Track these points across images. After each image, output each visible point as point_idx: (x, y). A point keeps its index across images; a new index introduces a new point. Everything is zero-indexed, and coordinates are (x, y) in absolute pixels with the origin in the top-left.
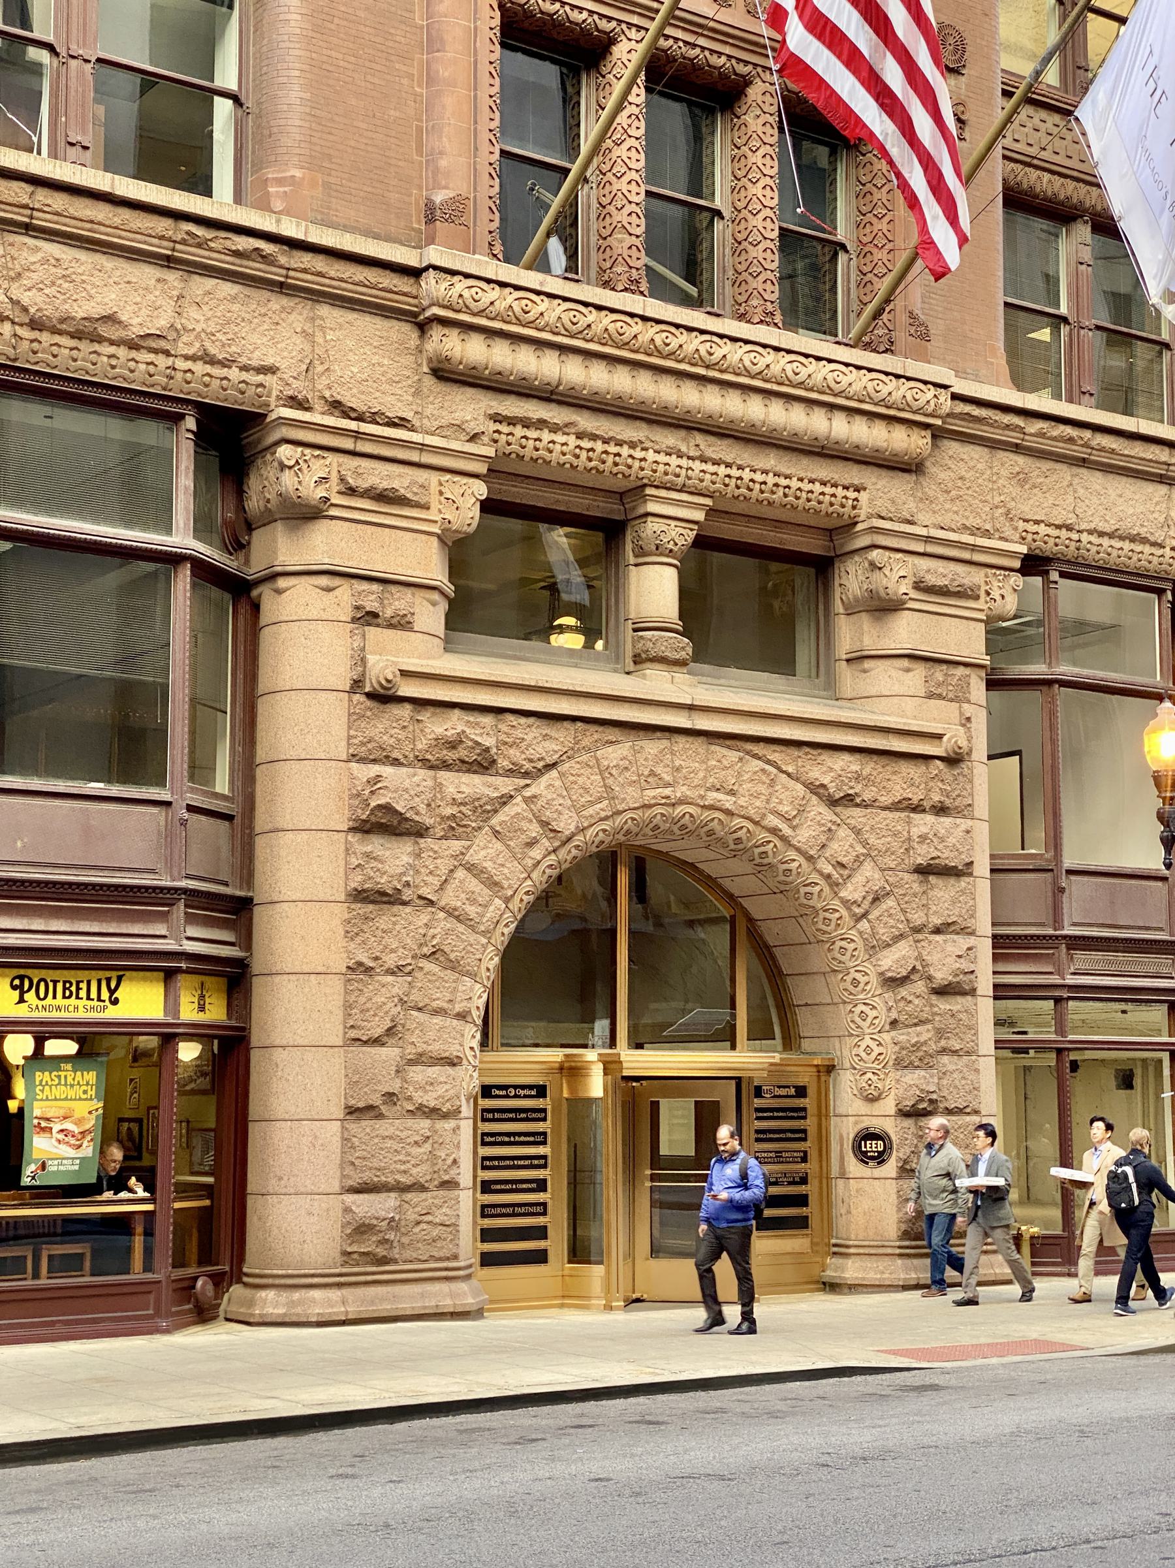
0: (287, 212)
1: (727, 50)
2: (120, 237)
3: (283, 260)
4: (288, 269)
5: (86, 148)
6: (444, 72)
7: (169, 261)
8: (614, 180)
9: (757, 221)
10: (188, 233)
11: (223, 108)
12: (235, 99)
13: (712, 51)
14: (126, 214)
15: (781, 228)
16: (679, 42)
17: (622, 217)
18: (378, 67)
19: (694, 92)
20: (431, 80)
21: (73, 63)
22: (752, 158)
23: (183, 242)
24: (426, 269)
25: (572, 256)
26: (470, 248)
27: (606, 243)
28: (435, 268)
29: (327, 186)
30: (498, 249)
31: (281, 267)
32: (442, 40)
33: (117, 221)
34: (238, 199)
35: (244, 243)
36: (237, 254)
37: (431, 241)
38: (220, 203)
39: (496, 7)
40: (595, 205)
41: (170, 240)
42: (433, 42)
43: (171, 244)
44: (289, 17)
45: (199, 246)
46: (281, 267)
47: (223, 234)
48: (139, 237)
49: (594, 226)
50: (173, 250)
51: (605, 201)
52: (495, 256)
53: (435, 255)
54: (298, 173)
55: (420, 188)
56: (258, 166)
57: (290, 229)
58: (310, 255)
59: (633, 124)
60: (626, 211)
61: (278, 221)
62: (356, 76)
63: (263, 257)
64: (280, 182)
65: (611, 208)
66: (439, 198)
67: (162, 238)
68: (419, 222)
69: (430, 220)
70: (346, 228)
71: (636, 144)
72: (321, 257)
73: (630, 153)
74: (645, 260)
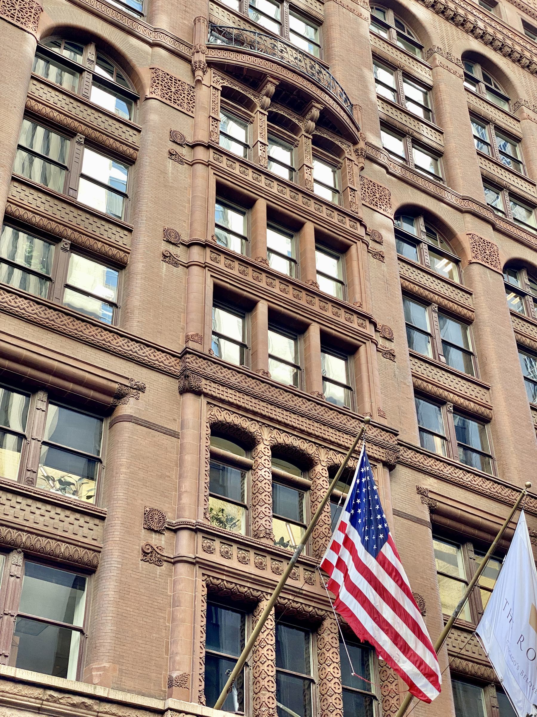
0: (101, 684)
1: (313, 604)
2: (16, 699)
3: (96, 707)
4: (98, 712)
5: (6, 656)
6: (180, 616)
7: (39, 711)
8: (261, 665)
9: (331, 685)
10: (50, 696)
11: (76, 636)
12: (81, 631)
13: (306, 605)
14: (20, 687)
15: (343, 688)
16: (287, 600)
17: (264, 683)
18: (149, 614)
19: (300, 623)
20: (173, 620)
21: (6, 617)
22: (327, 654)
23: (47, 700)
24: (167, 710)
25: (241, 703)
26: (189, 699)
27: (257, 696)
28: (171, 709)
29: (121, 670)
30: (203, 699)
31: (95, 711)
32: (180, 602)
33: (15, 691)
34: (78, 679)
35: (77, 700)
36: (73, 705)
37: (170, 696)
38: (70, 682)
39: (205, 586)
40: (252, 677)
41: (41, 699)
42: (175, 603)
43: (41, 702)
44: (109, 593)
45: (55, 702)
46: (95, 711)
47: (67, 696)
48: (25, 698)
49: (251, 688)
50: (42, 704)
51: (257, 675)
52: (201, 703)
53: (171, 703)
54: (107, 665)
55: (166, 670)
56: (88, 663)
57: (101, 692)
58: (110, 705)
59: (268, 638)
60: (266, 680)
61: (95, 688)
62: (138, 618)
63: (86, 706)
64: (98, 669)
65: (260, 679)
66: (175, 675)
67: (37, 698)
68: (165, 688)
69: (170, 686)
70: (129, 691)
71: (271, 647)
72: (115, 706)
73: (268, 652)
74: (276, 703)
